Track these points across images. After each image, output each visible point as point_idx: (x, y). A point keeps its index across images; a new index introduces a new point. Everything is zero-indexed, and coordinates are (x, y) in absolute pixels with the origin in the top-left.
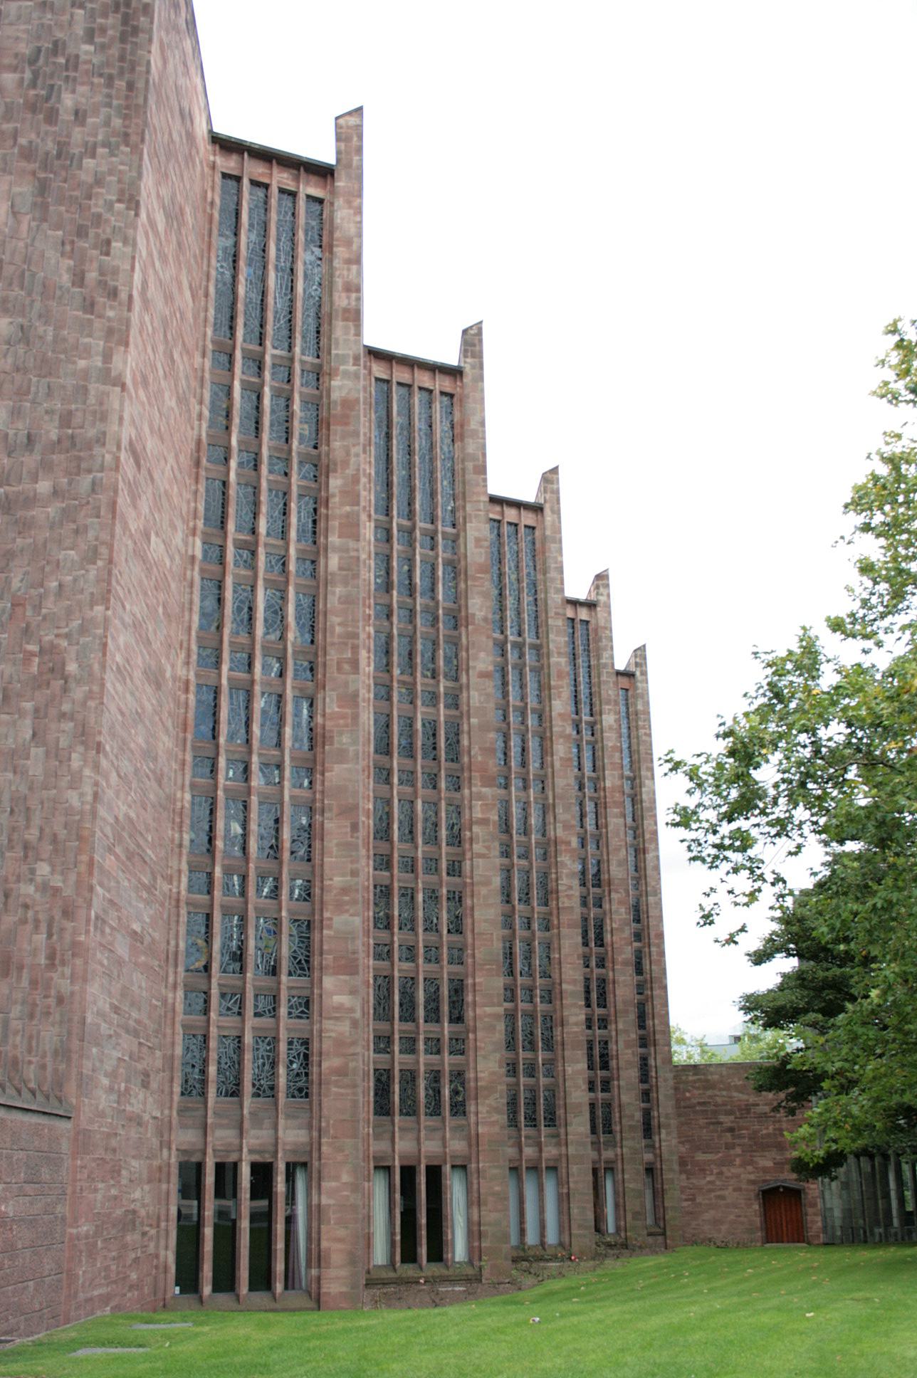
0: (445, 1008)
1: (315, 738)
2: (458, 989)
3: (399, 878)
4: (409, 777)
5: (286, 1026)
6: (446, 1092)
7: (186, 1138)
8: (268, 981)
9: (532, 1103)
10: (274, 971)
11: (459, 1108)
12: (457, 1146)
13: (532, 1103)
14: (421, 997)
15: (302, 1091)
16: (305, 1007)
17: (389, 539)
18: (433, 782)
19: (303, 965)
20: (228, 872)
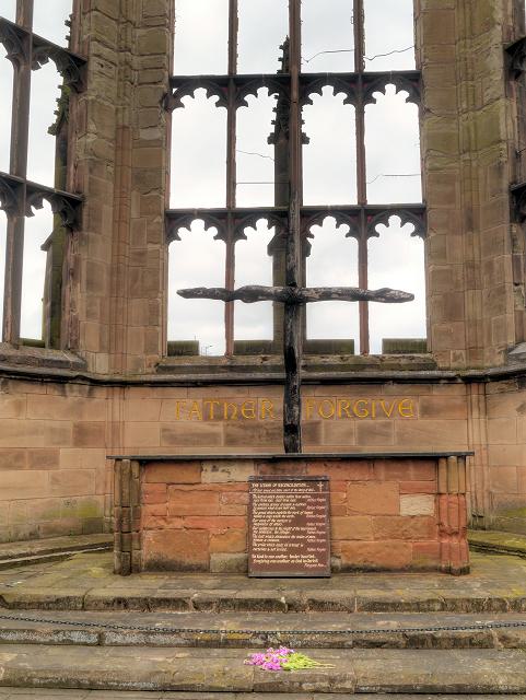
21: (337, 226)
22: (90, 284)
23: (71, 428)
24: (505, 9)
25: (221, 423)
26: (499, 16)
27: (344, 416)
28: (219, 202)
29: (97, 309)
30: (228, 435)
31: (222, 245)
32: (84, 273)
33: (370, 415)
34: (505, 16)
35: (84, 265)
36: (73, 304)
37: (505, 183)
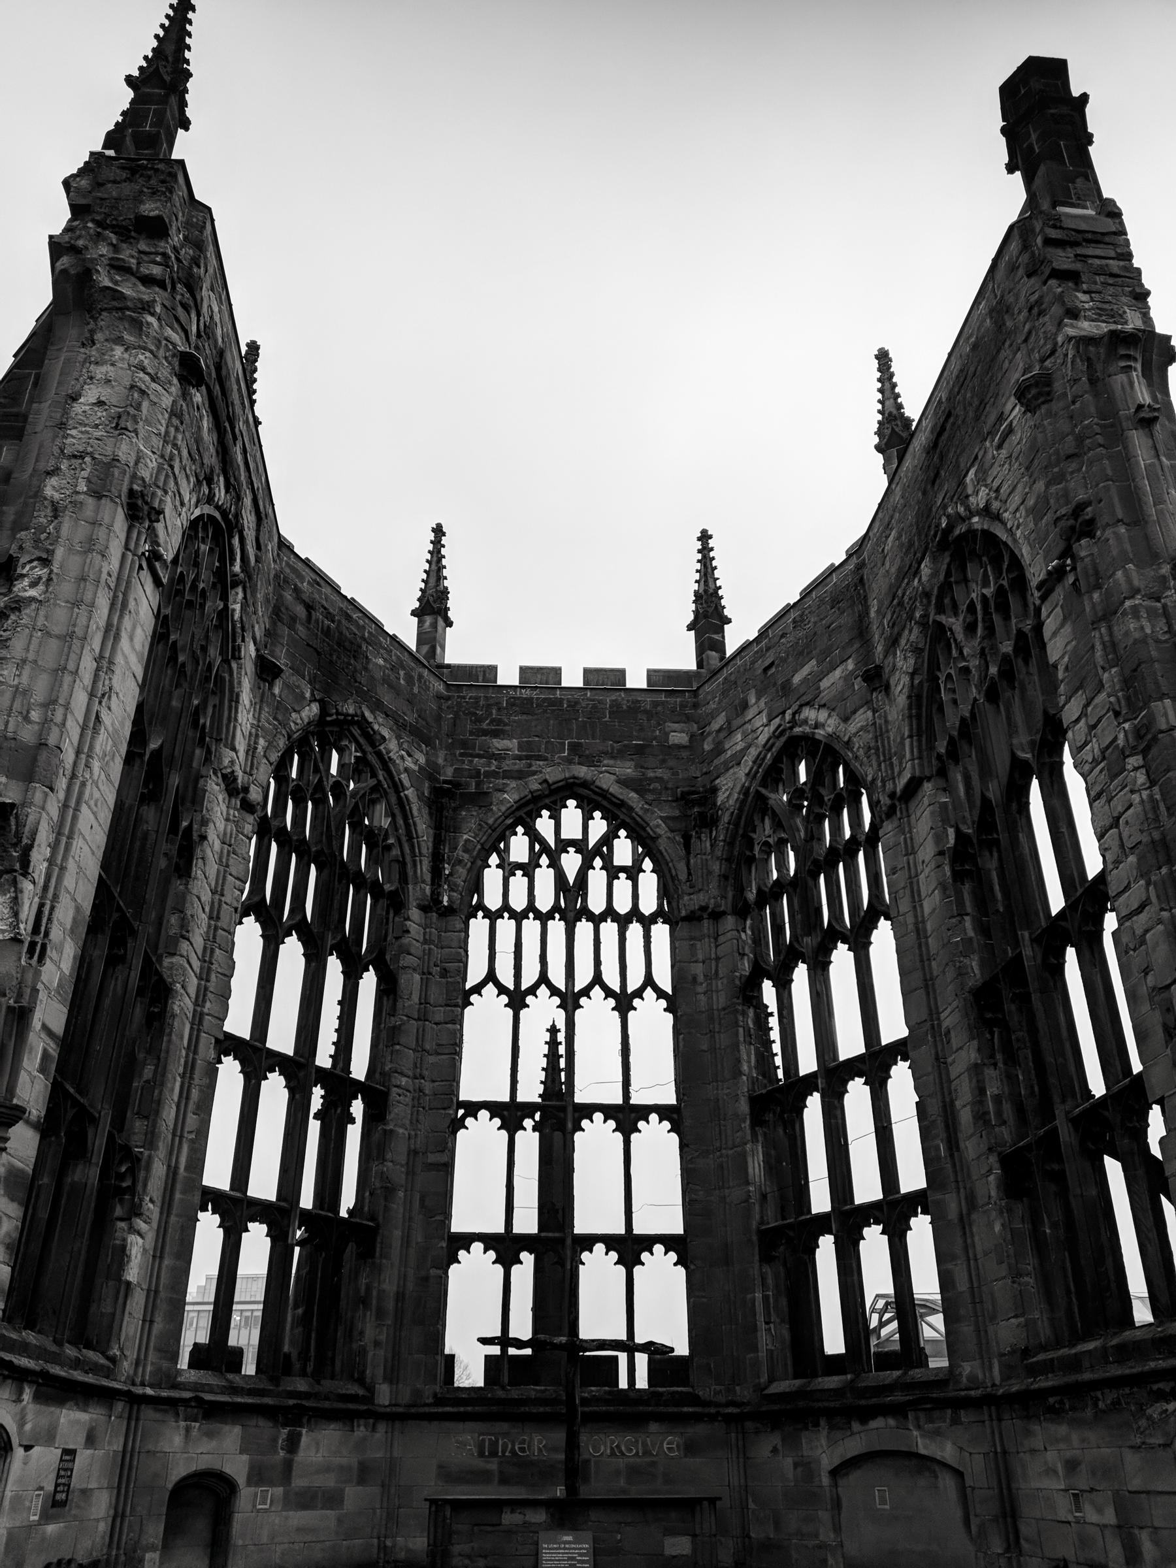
21: (607, 1254)
22: (380, 1314)
23: (356, 1465)
24: (749, 1062)
25: (495, 1460)
26: (745, 1068)
27: (613, 1454)
28: (497, 1226)
29: (383, 1337)
30: (501, 1472)
31: (499, 1269)
32: (374, 1302)
33: (637, 1453)
34: (750, 1067)
35: (375, 1293)
36: (362, 1333)
37: (754, 1225)
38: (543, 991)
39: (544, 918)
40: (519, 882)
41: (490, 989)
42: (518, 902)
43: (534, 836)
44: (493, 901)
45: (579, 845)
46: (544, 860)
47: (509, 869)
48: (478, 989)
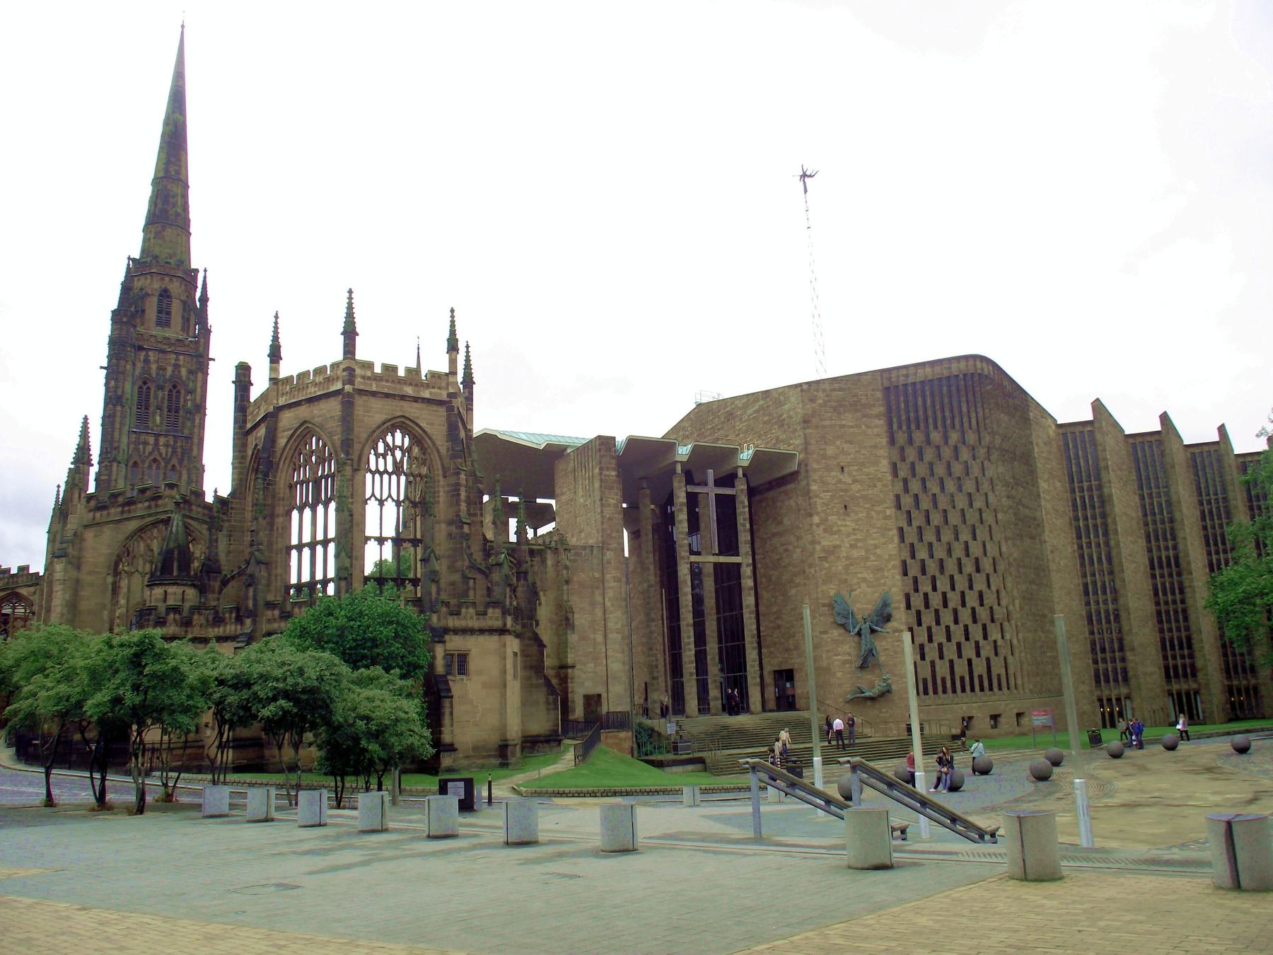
0: (1185, 645)
1: (1114, 591)
2: (1189, 639)
3: (1163, 608)
4: (1162, 576)
5: (1119, 665)
6: (1189, 671)
7: (1098, 693)
8: (1112, 655)
9: (1235, 667)
10: (1114, 652)
11: (1194, 675)
12: (1195, 686)
13: (1235, 667)
14: (1176, 643)
15: (1126, 679)
16: (1123, 660)
17: (1144, 499)
18: (1171, 575)
19: (1121, 649)
20: (1098, 629)
38: (390, 499)
39: (390, 474)
40: (381, 460)
41: (373, 498)
42: (381, 468)
43: (386, 445)
44: (373, 467)
45: (401, 448)
46: (389, 452)
47: (377, 455)
48: (369, 499)
